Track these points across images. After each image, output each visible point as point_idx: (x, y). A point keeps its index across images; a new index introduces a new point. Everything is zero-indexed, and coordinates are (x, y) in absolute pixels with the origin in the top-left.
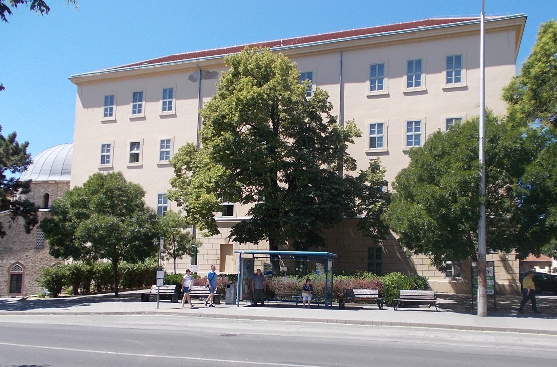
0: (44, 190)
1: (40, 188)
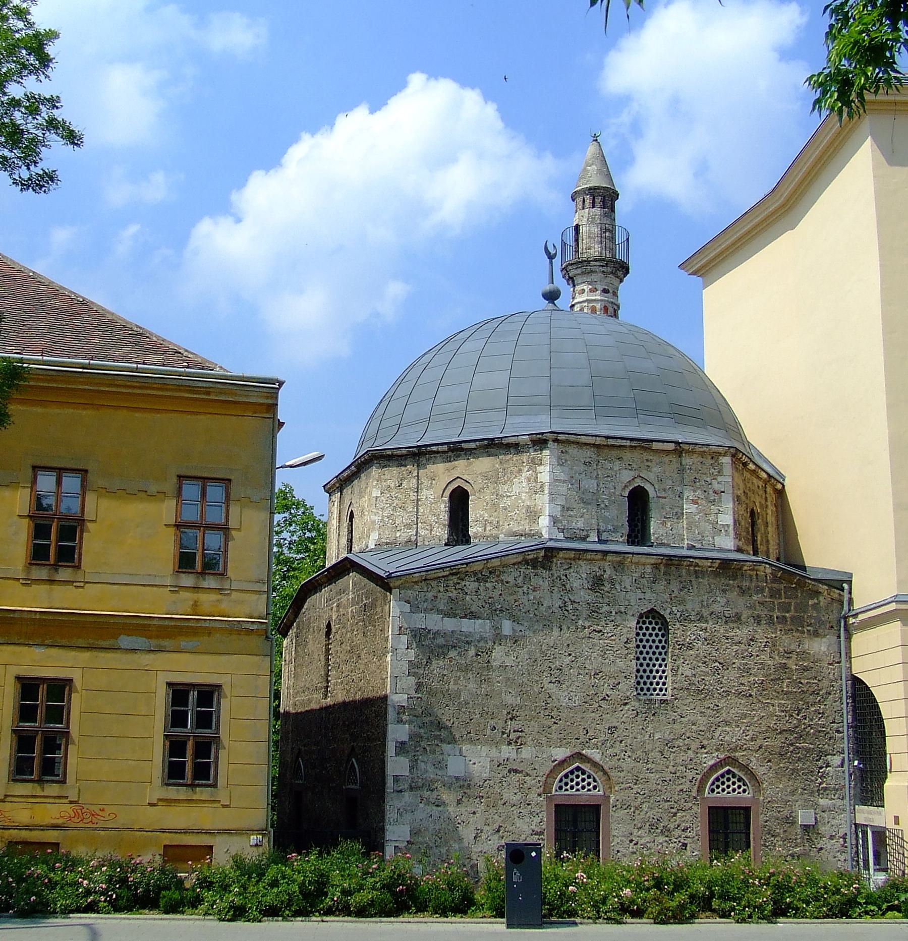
0: (632, 473)
1: (617, 465)
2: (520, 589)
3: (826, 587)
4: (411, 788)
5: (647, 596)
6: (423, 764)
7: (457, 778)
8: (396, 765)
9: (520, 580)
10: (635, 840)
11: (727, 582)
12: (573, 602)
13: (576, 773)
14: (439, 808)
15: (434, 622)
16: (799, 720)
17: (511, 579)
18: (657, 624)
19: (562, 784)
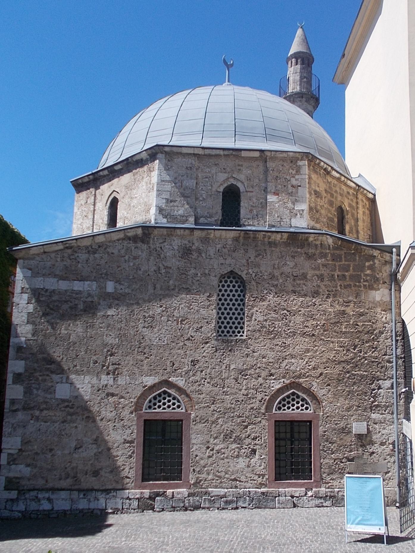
2: (122, 258)
3: (379, 252)
4: (24, 409)
5: (227, 262)
6: (34, 390)
7: (63, 401)
8: (14, 391)
9: (123, 252)
10: (211, 447)
11: (296, 249)
12: (166, 268)
13: (163, 396)
14: (49, 423)
15: (51, 284)
16: (355, 354)
17: (116, 251)
18: (237, 282)
19: (152, 404)
